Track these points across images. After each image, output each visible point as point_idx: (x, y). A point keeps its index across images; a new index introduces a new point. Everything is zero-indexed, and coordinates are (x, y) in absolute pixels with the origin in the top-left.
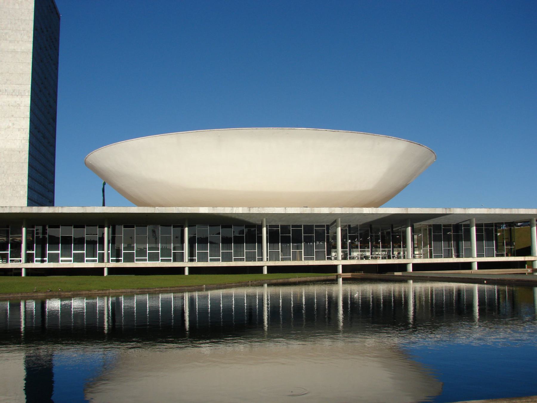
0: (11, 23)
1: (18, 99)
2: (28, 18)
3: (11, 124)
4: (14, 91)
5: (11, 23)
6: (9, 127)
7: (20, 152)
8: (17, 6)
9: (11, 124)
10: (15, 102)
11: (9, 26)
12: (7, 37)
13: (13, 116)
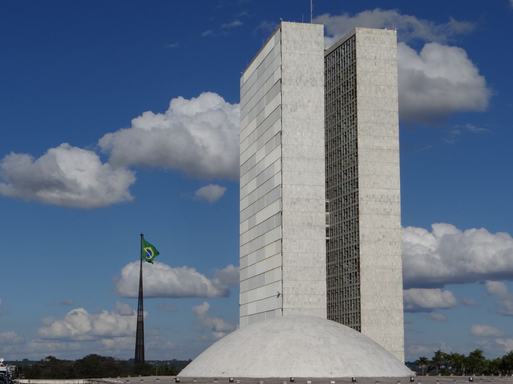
0: (375, 115)
1: (387, 206)
2: (392, 109)
3: (381, 237)
4: (382, 197)
5: (375, 115)
6: (379, 240)
7: (392, 270)
8: (380, 95)
9: (381, 237)
10: (385, 210)
11: (373, 118)
12: (371, 131)
13: (382, 226)
